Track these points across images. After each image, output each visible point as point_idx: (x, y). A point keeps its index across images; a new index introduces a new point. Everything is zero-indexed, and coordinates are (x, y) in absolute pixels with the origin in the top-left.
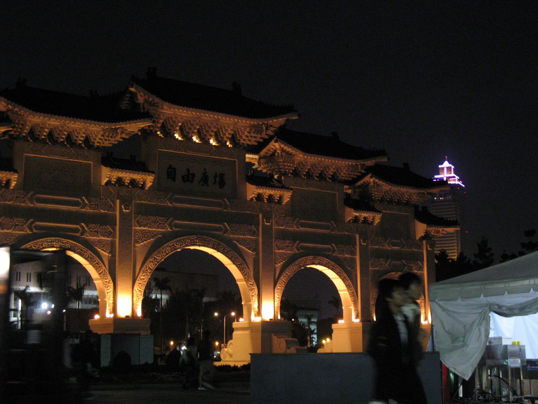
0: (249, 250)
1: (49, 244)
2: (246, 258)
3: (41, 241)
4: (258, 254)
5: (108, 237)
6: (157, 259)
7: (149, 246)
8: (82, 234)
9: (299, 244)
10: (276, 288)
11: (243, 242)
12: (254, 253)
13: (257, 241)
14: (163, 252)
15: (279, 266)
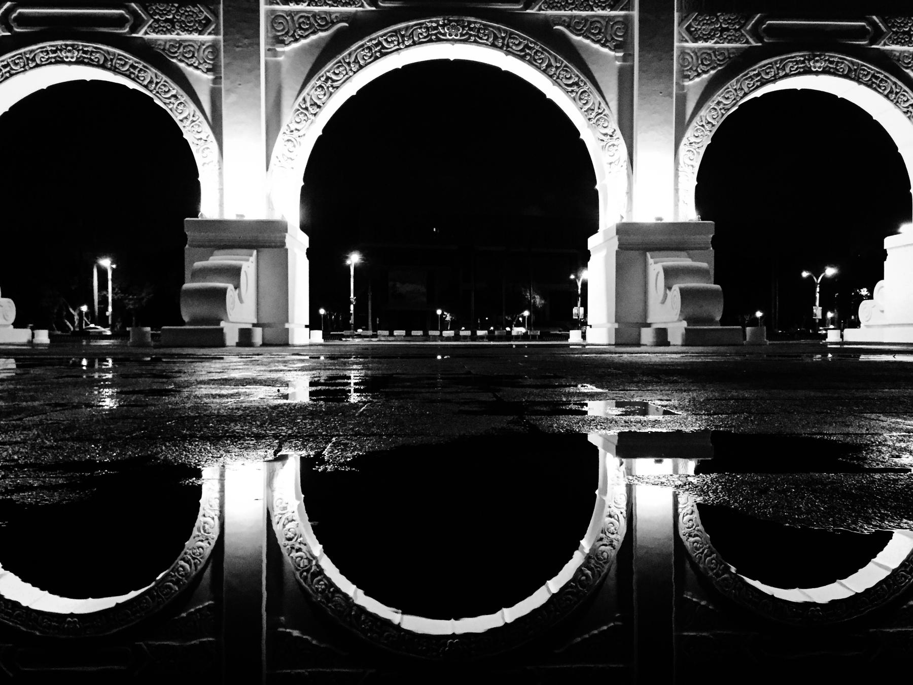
0: (603, 45)
1: (51, 55)
2: (593, 68)
3: (31, 52)
4: (628, 57)
5: (201, 33)
6: (334, 81)
7: (317, 53)
8: (134, 29)
9: (760, 22)
10: (685, 141)
11: (586, 27)
12: (621, 54)
13: (626, 22)
14: (349, 64)
15: (695, 85)
